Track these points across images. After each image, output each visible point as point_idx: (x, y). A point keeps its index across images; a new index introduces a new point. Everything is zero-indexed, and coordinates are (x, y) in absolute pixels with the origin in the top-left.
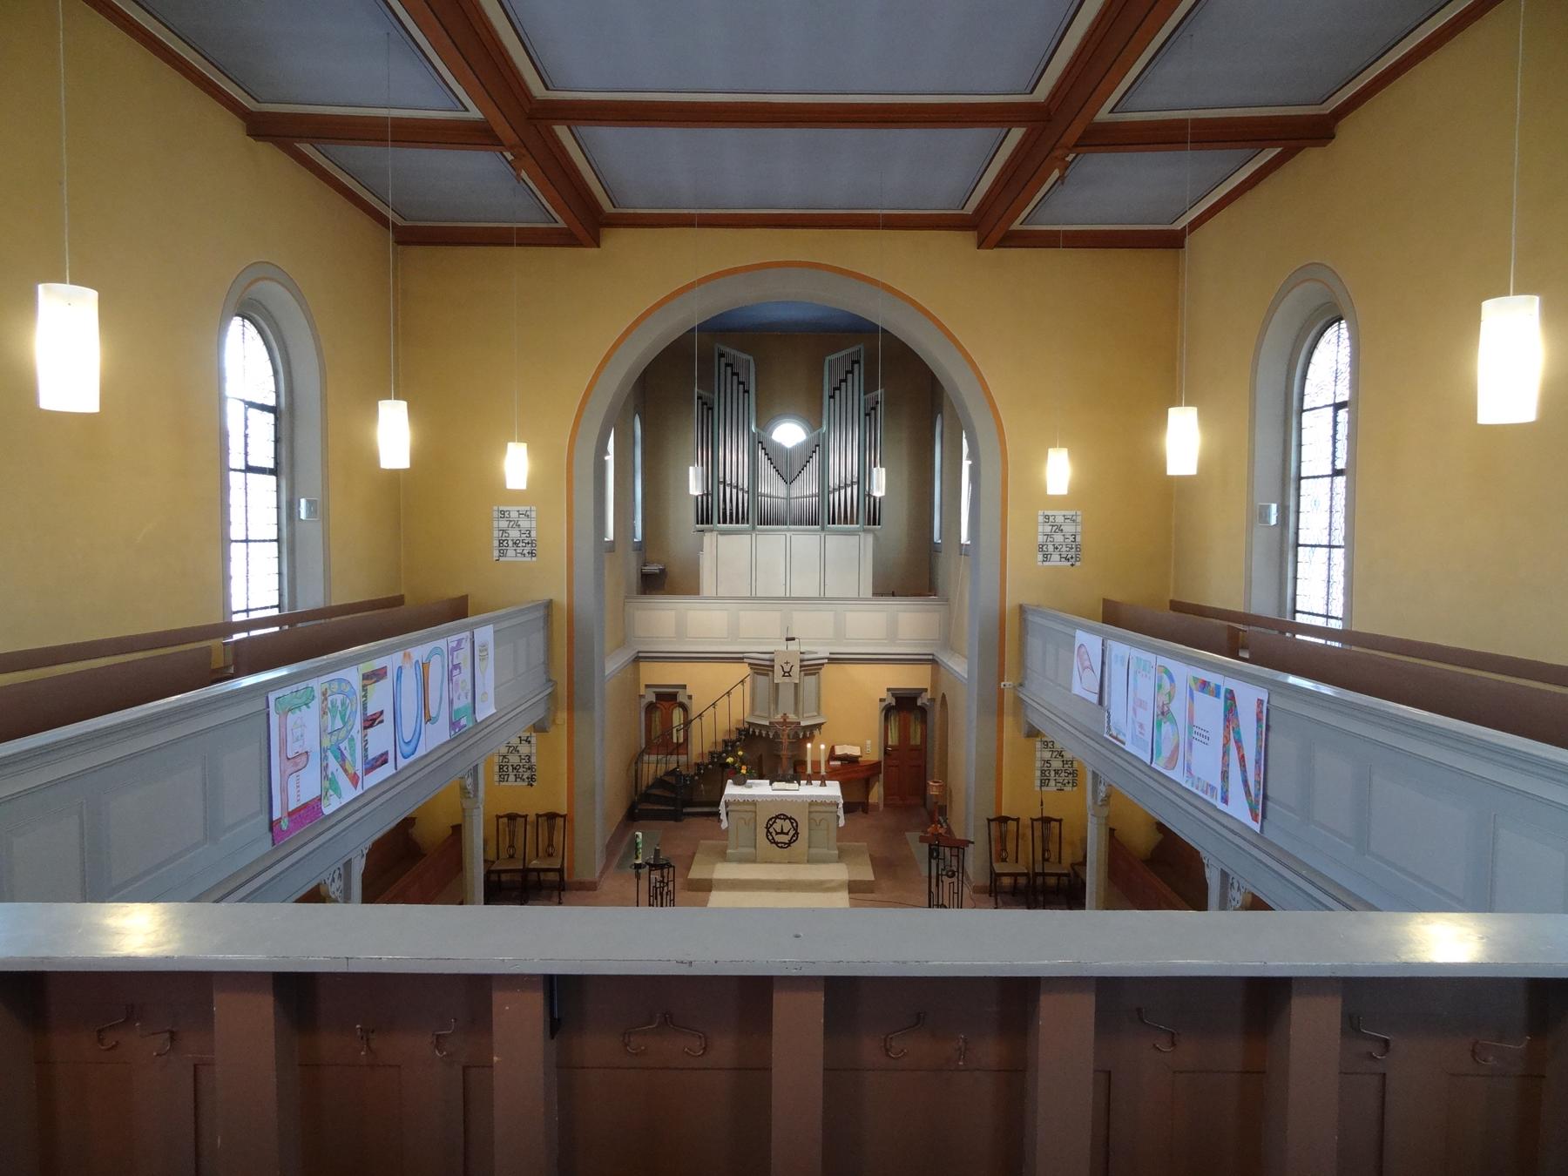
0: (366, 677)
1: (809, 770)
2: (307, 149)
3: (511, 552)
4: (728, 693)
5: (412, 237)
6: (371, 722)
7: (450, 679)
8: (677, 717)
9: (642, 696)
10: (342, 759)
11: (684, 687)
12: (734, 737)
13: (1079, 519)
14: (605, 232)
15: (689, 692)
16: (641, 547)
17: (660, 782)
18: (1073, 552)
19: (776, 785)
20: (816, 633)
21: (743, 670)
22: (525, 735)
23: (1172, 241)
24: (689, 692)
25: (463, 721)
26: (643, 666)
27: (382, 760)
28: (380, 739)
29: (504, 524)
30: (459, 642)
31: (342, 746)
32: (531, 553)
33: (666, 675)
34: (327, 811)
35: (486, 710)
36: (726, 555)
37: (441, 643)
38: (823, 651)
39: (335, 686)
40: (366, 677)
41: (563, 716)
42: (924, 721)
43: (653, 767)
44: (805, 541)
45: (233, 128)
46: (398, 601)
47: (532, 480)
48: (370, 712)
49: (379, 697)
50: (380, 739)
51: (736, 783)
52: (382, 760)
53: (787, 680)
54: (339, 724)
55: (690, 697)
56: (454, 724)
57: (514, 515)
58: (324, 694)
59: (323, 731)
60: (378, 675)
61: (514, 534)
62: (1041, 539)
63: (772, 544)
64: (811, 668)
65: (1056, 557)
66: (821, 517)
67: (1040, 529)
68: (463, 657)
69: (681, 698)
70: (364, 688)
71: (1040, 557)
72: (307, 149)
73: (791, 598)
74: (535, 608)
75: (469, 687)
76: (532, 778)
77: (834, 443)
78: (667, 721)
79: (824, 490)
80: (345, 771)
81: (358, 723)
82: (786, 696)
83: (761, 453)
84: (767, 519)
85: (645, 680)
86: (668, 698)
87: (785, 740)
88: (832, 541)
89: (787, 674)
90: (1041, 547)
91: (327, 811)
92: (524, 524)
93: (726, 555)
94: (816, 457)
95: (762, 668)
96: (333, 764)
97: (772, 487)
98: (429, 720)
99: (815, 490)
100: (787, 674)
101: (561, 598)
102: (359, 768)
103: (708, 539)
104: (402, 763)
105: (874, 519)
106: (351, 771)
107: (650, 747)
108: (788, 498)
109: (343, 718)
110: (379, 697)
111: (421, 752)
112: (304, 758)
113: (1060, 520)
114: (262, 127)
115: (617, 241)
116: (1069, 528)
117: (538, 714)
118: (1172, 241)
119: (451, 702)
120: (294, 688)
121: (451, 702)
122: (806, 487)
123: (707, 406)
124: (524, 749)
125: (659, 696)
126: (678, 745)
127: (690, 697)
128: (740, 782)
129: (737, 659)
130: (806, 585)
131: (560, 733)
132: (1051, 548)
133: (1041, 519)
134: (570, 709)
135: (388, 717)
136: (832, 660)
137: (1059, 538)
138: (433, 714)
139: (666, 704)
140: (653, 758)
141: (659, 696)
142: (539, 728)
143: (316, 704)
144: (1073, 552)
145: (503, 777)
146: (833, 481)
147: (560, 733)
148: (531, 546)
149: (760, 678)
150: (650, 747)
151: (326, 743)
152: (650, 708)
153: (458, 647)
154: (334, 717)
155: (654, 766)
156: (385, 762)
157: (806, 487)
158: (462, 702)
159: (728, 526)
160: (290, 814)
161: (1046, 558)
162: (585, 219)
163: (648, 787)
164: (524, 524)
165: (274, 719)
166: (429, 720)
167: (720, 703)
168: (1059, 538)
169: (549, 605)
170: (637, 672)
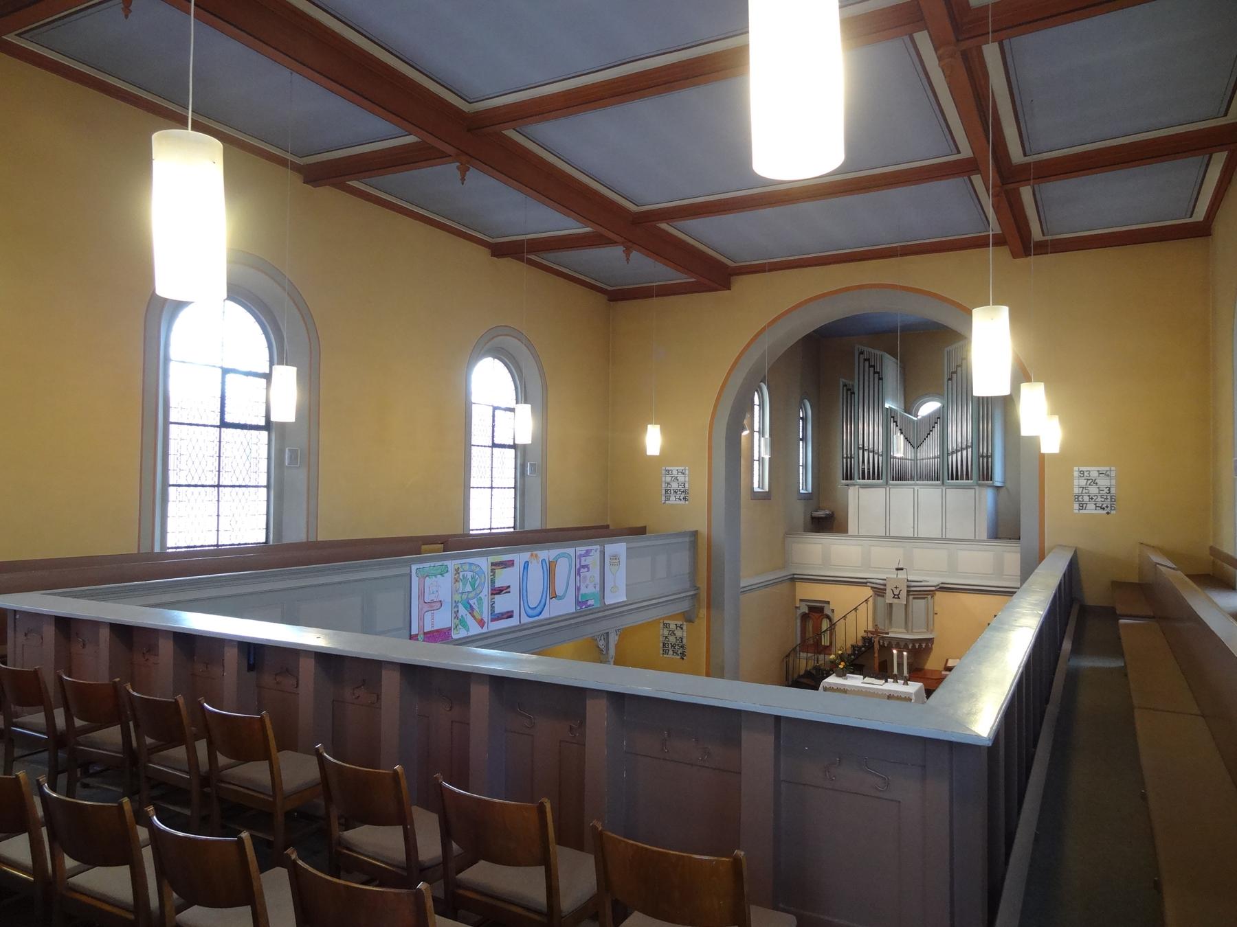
0: (492, 564)
1: (895, 672)
2: (532, 257)
3: (672, 498)
4: (856, 609)
5: (619, 295)
6: (499, 591)
7: (578, 573)
8: (825, 625)
10: (471, 610)
11: (828, 603)
12: (860, 644)
13: (1113, 474)
14: (733, 278)
15: (832, 606)
16: (807, 498)
18: (1108, 502)
19: (868, 679)
20: (929, 567)
21: (867, 592)
22: (679, 623)
23: (1202, 231)
24: (832, 606)
25: (590, 602)
26: (798, 584)
27: (509, 615)
28: (503, 603)
29: (668, 479)
30: (588, 552)
32: (685, 499)
33: (817, 593)
34: (455, 636)
35: (617, 595)
36: (864, 502)
37: (571, 551)
38: (935, 580)
39: (467, 567)
40: (492, 564)
41: (703, 612)
43: (803, 662)
44: (929, 494)
45: (484, 253)
46: (607, 527)
47: (662, 451)
48: (497, 585)
49: (504, 577)
50: (503, 603)
51: (839, 676)
52: (509, 615)
53: (896, 601)
56: (578, 603)
57: (675, 473)
58: (457, 571)
59: (454, 591)
60: (510, 564)
61: (675, 485)
62: (1077, 491)
63: (902, 495)
64: (918, 593)
65: (1091, 506)
66: (945, 474)
67: (1076, 482)
68: (593, 560)
69: (827, 611)
70: (493, 571)
71: (1076, 506)
72: (532, 257)
73: (918, 538)
74: (684, 534)
75: (597, 579)
76: (683, 654)
77: (952, 415)
78: (817, 628)
79: (944, 452)
81: (486, 591)
82: (899, 614)
83: (893, 425)
84: (901, 476)
86: (817, 611)
87: (876, 646)
88: (952, 494)
89: (897, 596)
90: (1077, 498)
91: (455, 636)
92: (681, 479)
93: (864, 502)
94: (937, 427)
95: (879, 591)
96: (463, 611)
97: (900, 447)
99: (937, 453)
100: (897, 596)
101: (704, 530)
102: (486, 617)
103: (852, 492)
104: (525, 620)
105: (987, 475)
106: (478, 617)
107: (804, 646)
108: (915, 459)
109: (473, 586)
110: (504, 577)
112: (438, 605)
113: (1094, 474)
114: (501, 250)
115: (741, 284)
116: (1103, 482)
117: (684, 606)
118: (1202, 231)
119: (578, 589)
121: (578, 589)
122: (930, 451)
123: (850, 391)
124: (679, 633)
125: (811, 609)
126: (826, 647)
128: (842, 674)
129: (862, 583)
130: (930, 528)
131: (701, 623)
132: (1086, 499)
133: (1076, 474)
134: (708, 607)
135: (515, 590)
136: (943, 588)
137: (1093, 490)
138: (559, 592)
140: (803, 655)
141: (811, 609)
142: (688, 617)
143: (449, 577)
144: (1108, 502)
145: (665, 651)
146: (951, 446)
147: (701, 623)
148: (685, 494)
149: (879, 599)
150: (804, 646)
151: (457, 597)
152: (805, 617)
153: (588, 553)
154: (465, 585)
156: (511, 616)
157: (930, 451)
158: (590, 589)
159: (866, 481)
160: (425, 633)
161: (1082, 506)
162: (713, 274)
163: (800, 676)
164: (681, 479)
165: (415, 580)
167: (853, 618)
168: (1093, 490)
169: (695, 534)
170: (793, 590)
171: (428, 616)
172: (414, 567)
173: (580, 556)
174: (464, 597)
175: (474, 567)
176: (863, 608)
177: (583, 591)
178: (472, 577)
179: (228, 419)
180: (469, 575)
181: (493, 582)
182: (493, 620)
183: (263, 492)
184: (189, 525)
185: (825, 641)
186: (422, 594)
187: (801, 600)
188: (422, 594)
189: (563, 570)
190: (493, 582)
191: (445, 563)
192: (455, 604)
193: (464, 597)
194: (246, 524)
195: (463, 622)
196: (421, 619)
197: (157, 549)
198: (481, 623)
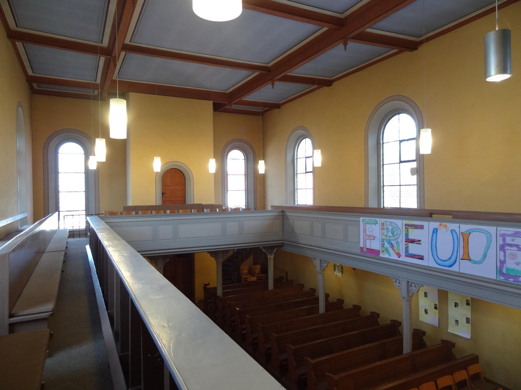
0: (406, 225)
6: (413, 241)
10: (392, 246)
27: (421, 258)
28: (413, 249)
31: (392, 242)
34: (382, 255)
39: (389, 224)
40: (406, 225)
49: (414, 234)
50: (413, 249)
52: (421, 258)
54: (390, 234)
56: (500, 271)
58: (383, 224)
60: (422, 227)
70: (406, 228)
80: (394, 250)
81: (402, 239)
96: (387, 245)
98: (467, 257)
106: (396, 251)
109: (393, 234)
111: (455, 268)
112: (373, 238)
120: (370, 219)
151: (384, 237)
165: (361, 224)
166: (467, 257)
171: (368, 241)
172: (361, 219)
173: (504, 236)
174: (388, 238)
175: (393, 224)
177: (510, 264)
178: (392, 229)
179: (402, 160)
180: (390, 228)
181: (407, 235)
182: (406, 256)
183: (415, 188)
184: (390, 201)
186: (365, 231)
188: (365, 231)
189: (473, 239)
190: (407, 235)
191: (377, 219)
192: (383, 240)
193: (388, 238)
194: (410, 201)
195: (387, 250)
196: (365, 242)
197: (382, 207)
198: (399, 255)
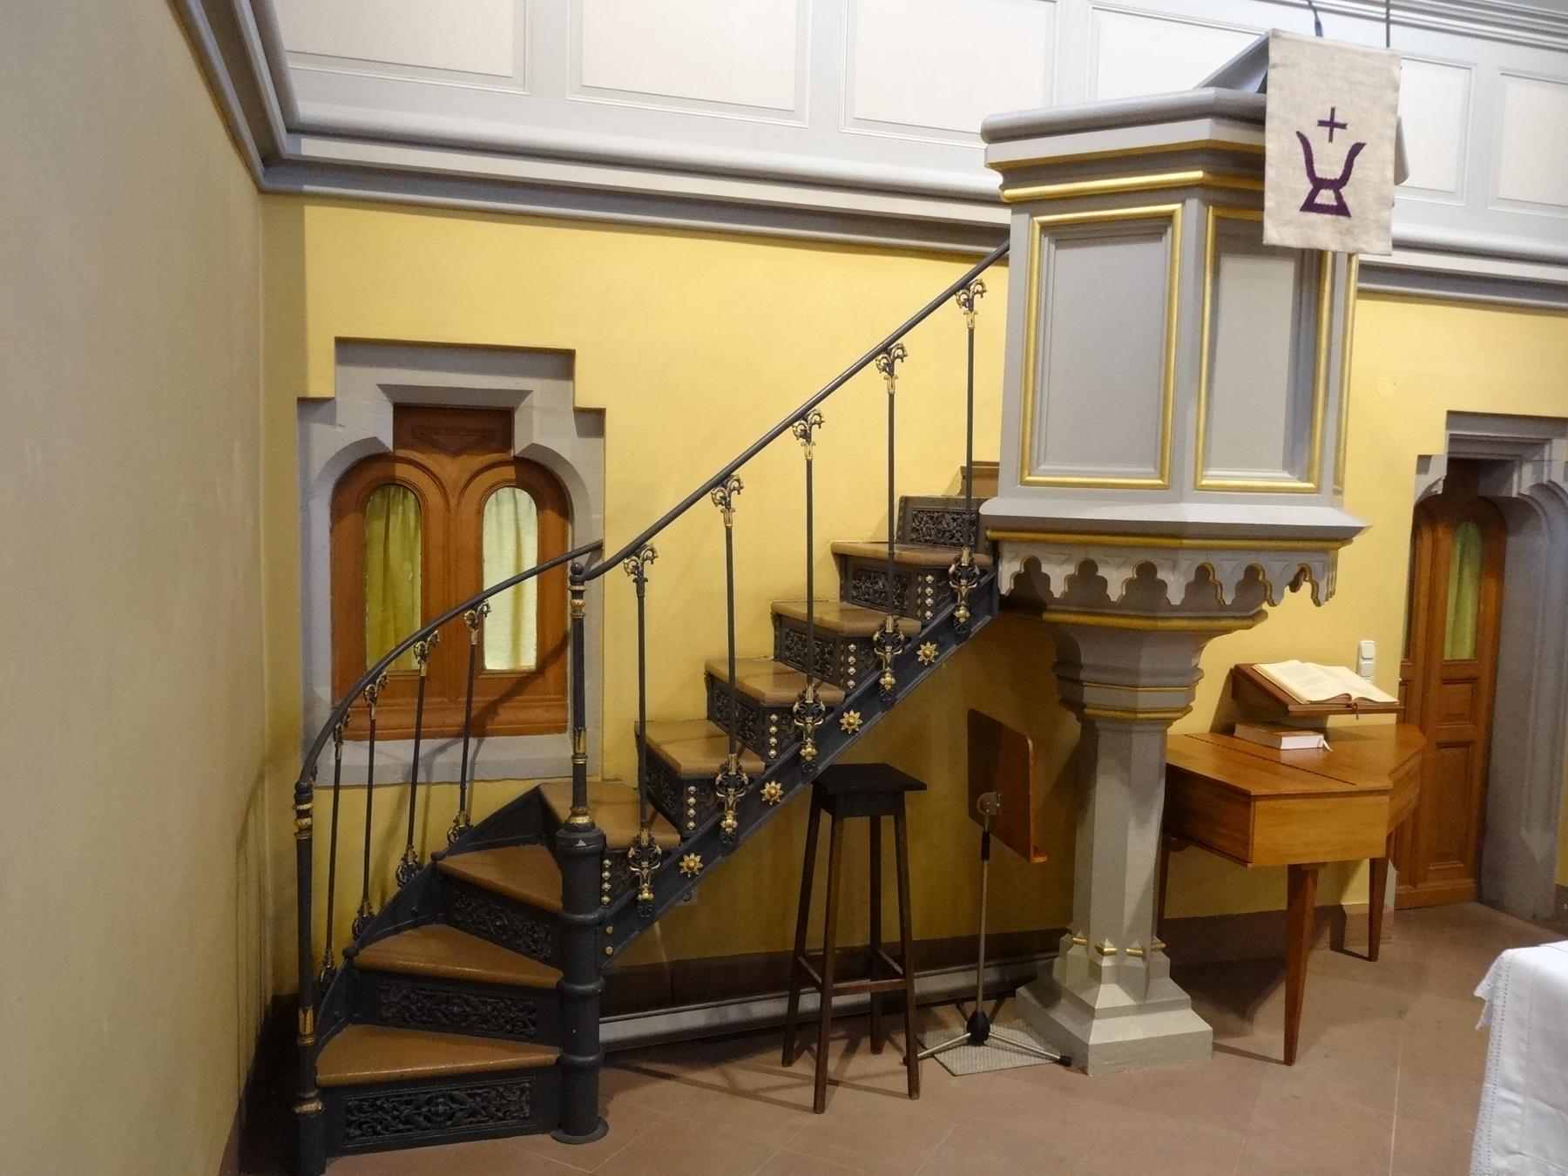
9: (308, 405)
11: (561, 363)
15: (588, 389)
17: (432, 894)
24: (588, 389)
26: (334, 233)
42: (1493, 566)
55: (592, 421)
69: (542, 427)
85: (330, 317)
86: (465, 428)
125: (419, 418)
127: (592, 421)
139: (451, 468)
152: (364, 481)
155: (392, 805)
163: (368, 929)
176: (933, 353)
185: (508, 641)
187: (350, 349)
